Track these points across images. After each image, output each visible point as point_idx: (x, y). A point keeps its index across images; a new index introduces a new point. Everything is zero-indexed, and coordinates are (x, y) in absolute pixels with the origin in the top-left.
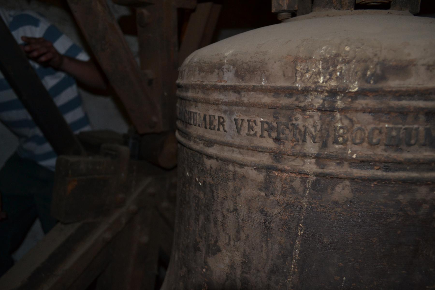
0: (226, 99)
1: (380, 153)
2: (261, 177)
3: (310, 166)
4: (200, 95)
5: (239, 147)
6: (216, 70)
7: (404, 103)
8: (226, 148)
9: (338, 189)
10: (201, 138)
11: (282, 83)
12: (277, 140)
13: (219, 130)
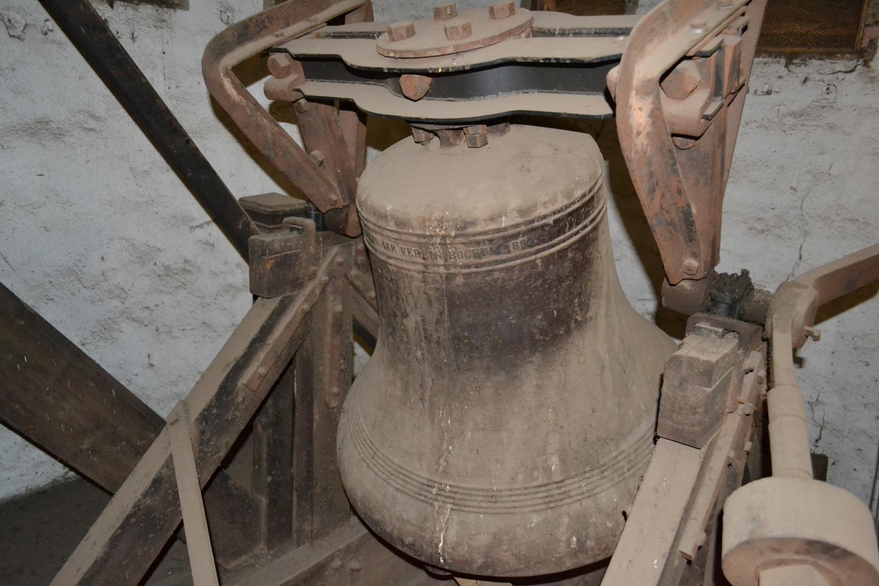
1: (472, 261)
2: (421, 276)
3: (442, 270)
4: (378, 230)
7: (477, 238)
9: (458, 279)
10: (383, 254)
12: (424, 258)
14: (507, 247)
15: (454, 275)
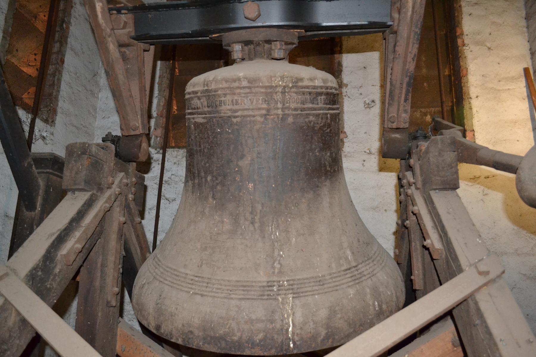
0: (244, 92)
1: (299, 105)
3: (280, 112)
5: (252, 109)
6: (237, 82)
7: (303, 90)
8: (245, 111)
9: (289, 119)
11: (267, 84)
13: (241, 104)
14: (317, 100)
15: (288, 115)
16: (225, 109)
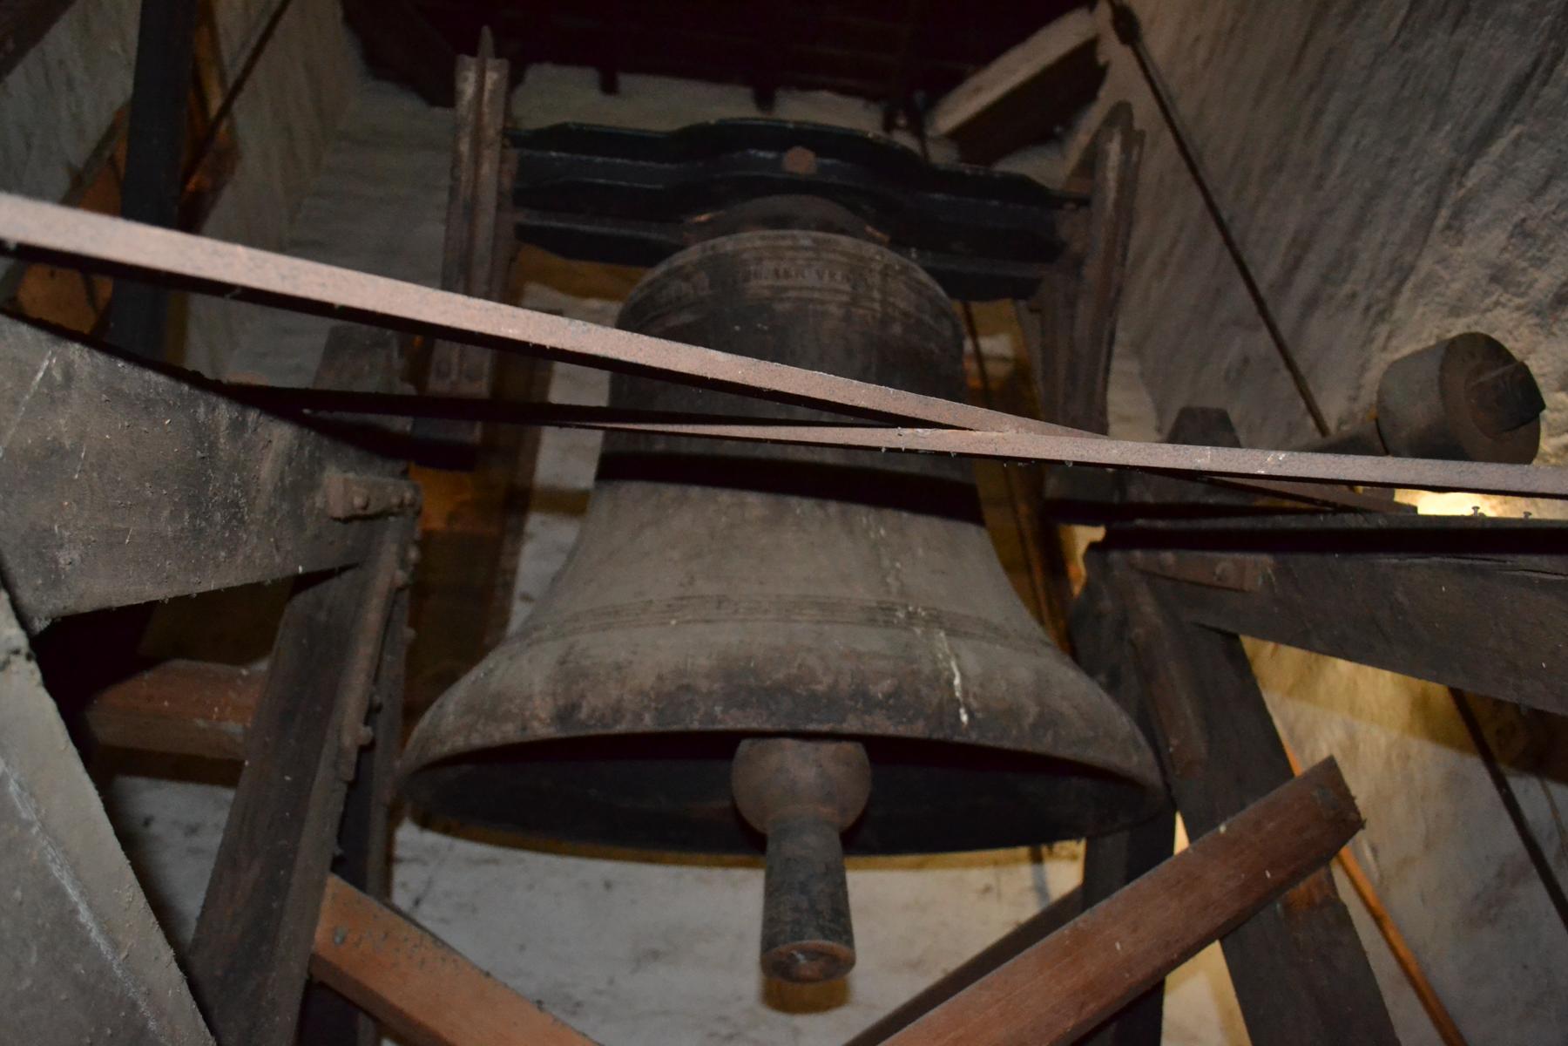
5: (820, 290)
16: (760, 285)
